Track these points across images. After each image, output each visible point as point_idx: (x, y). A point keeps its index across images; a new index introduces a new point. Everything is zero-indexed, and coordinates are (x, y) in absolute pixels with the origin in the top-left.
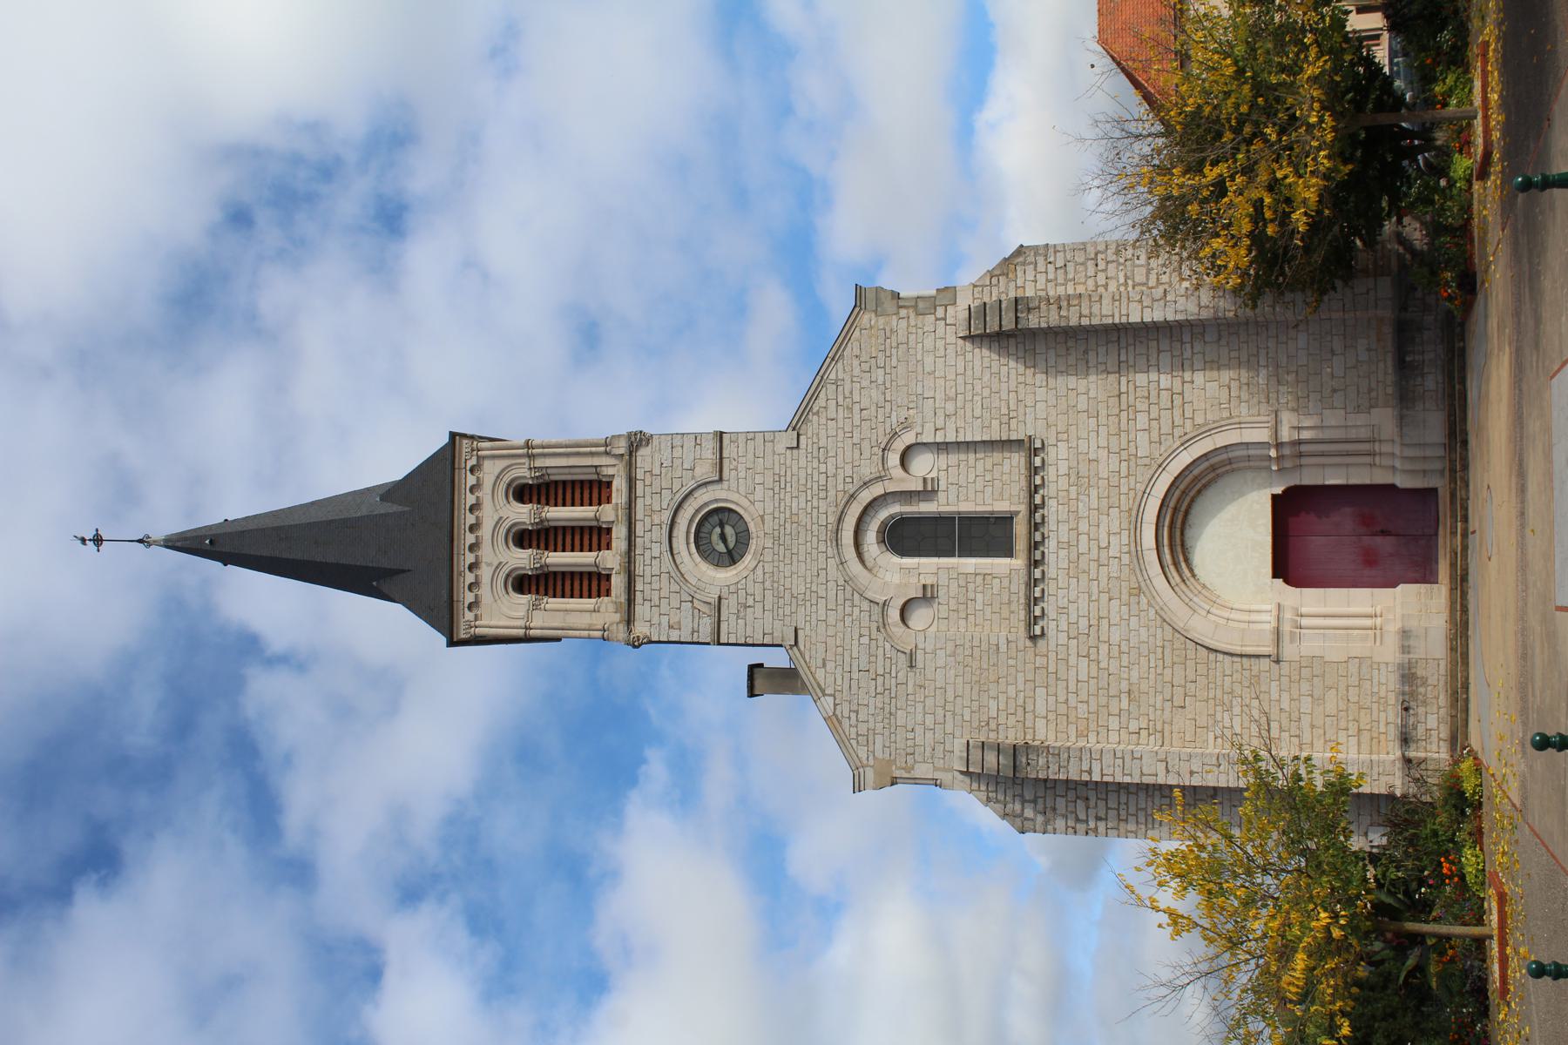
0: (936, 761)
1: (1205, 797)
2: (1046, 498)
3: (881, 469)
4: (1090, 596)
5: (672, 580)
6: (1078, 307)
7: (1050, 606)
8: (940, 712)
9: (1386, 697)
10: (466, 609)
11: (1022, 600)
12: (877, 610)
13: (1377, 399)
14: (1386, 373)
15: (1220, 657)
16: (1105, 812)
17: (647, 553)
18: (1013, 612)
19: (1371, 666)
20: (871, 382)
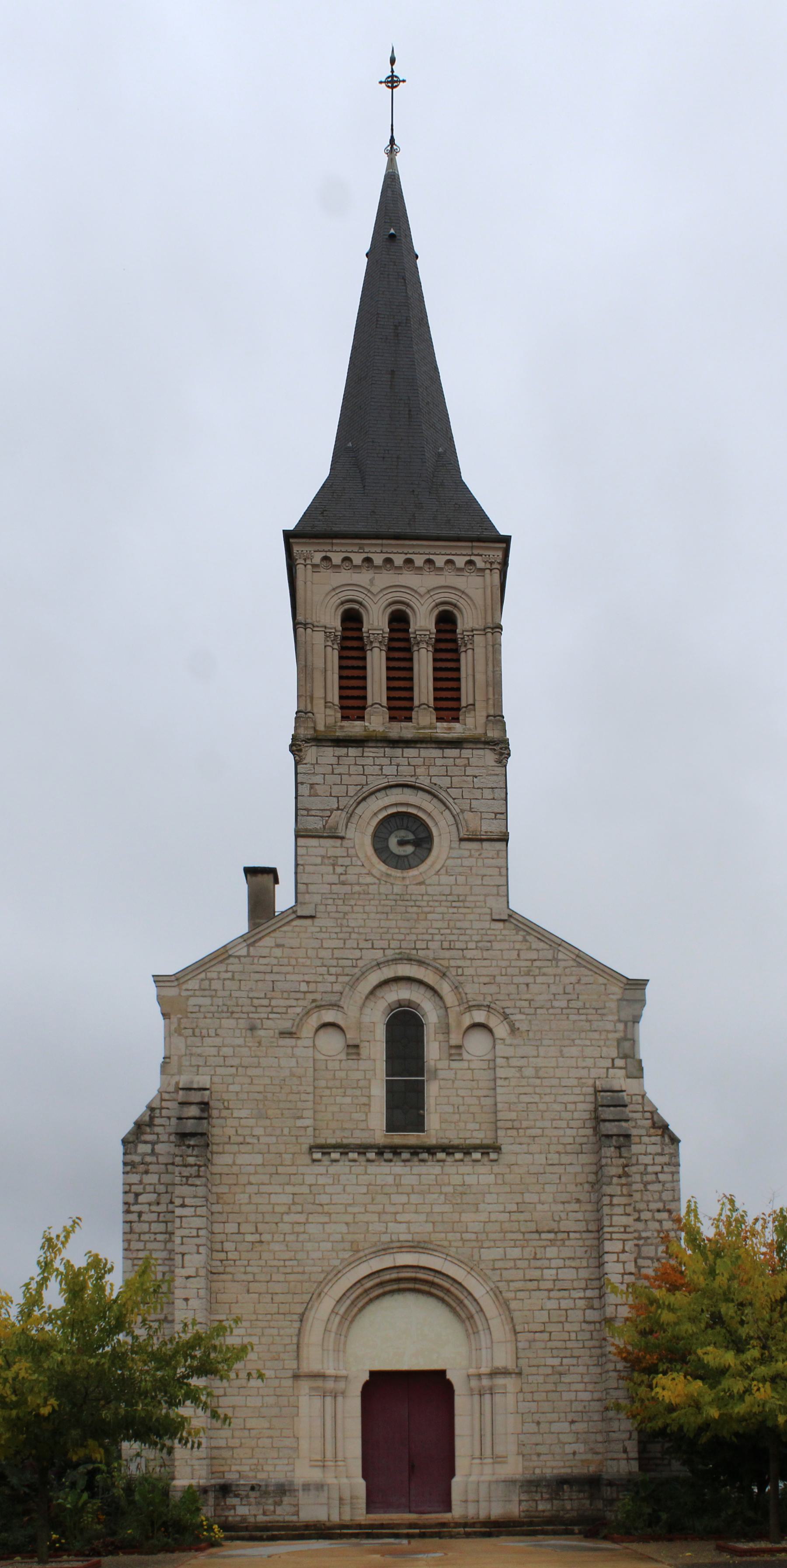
0: (188, 1058)
1: (165, 1312)
2: (441, 1164)
3: (471, 1003)
4: (350, 1205)
5: (359, 787)
8: (236, 1062)
11: (345, 1141)
12: (334, 998)
13: (531, 1460)
14: (553, 1468)
17: (386, 761)
18: (334, 1132)
20: (554, 995)
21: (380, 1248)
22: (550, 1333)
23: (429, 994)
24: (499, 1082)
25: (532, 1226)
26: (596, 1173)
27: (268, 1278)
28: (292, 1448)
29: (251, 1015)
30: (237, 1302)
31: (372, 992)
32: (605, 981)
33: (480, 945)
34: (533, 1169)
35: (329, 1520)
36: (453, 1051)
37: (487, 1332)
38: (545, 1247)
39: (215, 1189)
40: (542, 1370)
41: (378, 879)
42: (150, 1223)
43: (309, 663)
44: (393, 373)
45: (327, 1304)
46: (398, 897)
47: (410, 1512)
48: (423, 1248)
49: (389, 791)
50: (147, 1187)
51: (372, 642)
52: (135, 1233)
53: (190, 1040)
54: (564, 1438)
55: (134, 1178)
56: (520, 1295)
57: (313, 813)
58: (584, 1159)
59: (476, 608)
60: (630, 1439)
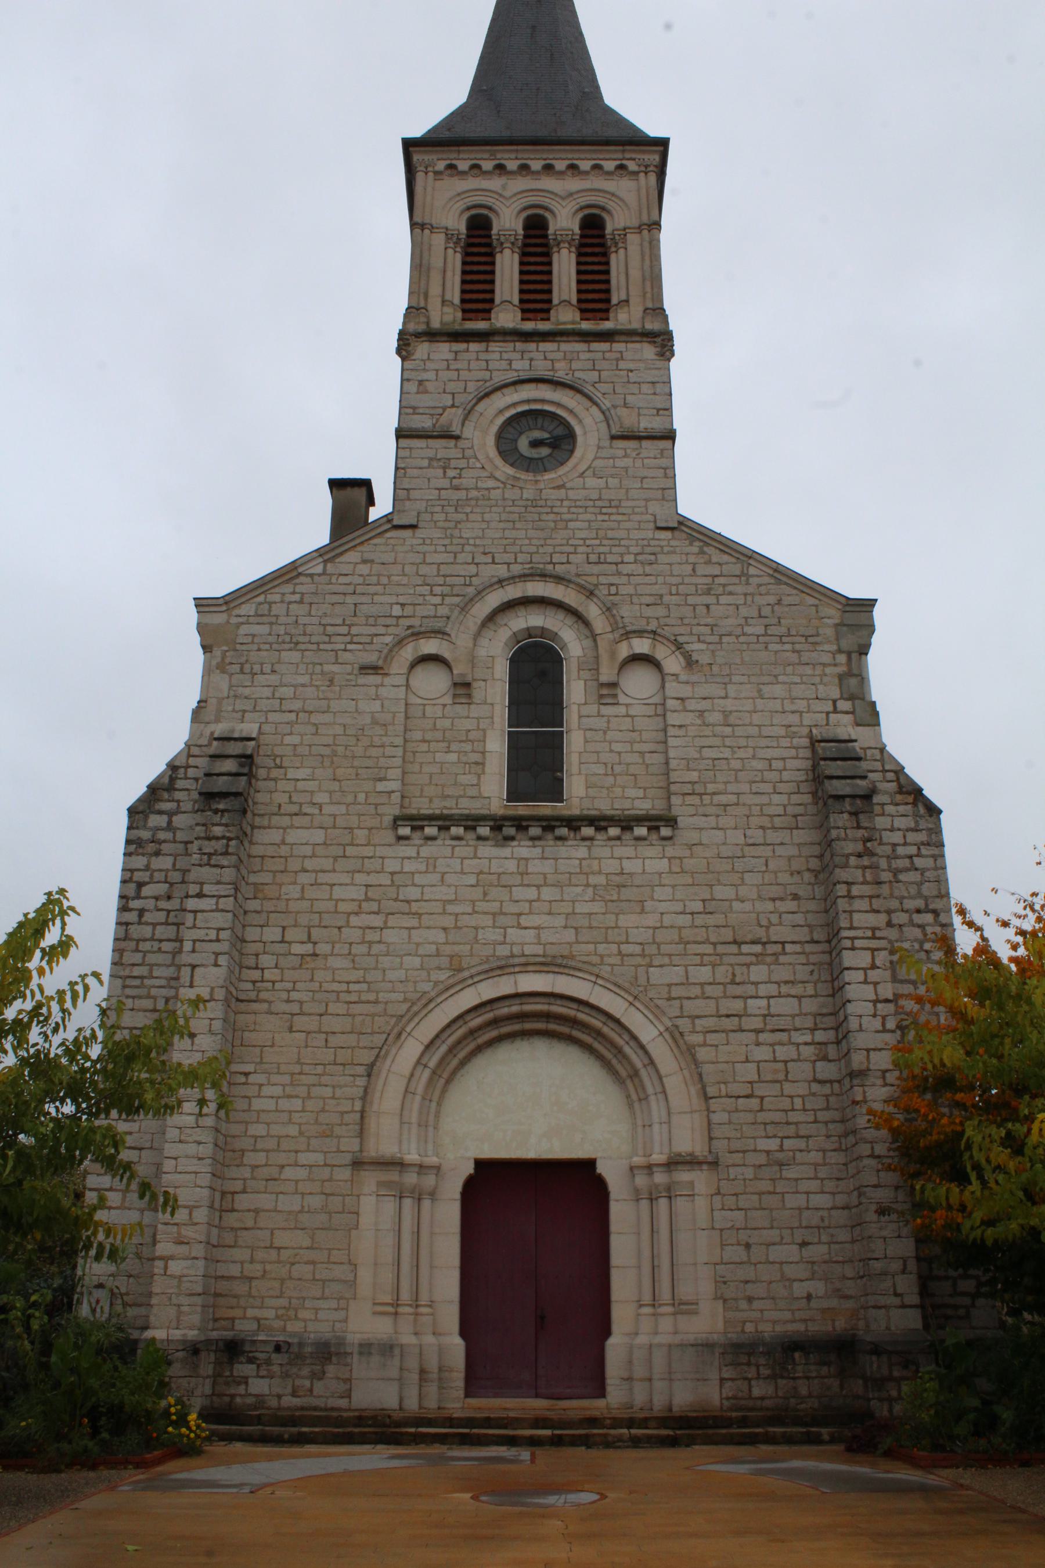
0: (231, 700)
2: (588, 843)
3: (628, 629)
4: (450, 902)
5: (481, 383)
6: (861, 879)
7: (440, 848)
8: (297, 705)
9: (296, 1318)
10: (448, 162)
12: (438, 624)
13: (737, 1309)
14: (774, 1322)
15: (361, 1082)
16: (150, 921)
17: (518, 356)
18: (431, 801)
19: (342, 1298)
20: (746, 618)
21: (494, 965)
22: (762, 1098)
23: (570, 620)
24: (671, 731)
25: (727, 935)
26: (821, 857)
27: (322, 1010)
28: (345, 1282)
29: (322, 646)
30: (272, 1046)
31: (491, 618)
32: (817, 602)
33: (640, 558)
34: (726, 851)
35: (401, 1409)
36: (605, 691)
37: (661, 1096)
38: (748, 965)
39: (252, 879)
40: (752, 1159)
41: (503, 483)
42: (154, 925)
43: (425, 262)
44: (534, 27)
45: (411, 1050)
46: (529, 503)
47: (537, 1396)
48: (560, 966)
49: (519, 387)
50: (156, 874)
51: (502, 244)
52: (131, 939)
53: (237, 679)
54: (790, 1271)
55: (140, 862)
56: (711, 1038)
57: (421, 411)
58: (800, 836)
59: (629, 209)
60: (903, 1272)
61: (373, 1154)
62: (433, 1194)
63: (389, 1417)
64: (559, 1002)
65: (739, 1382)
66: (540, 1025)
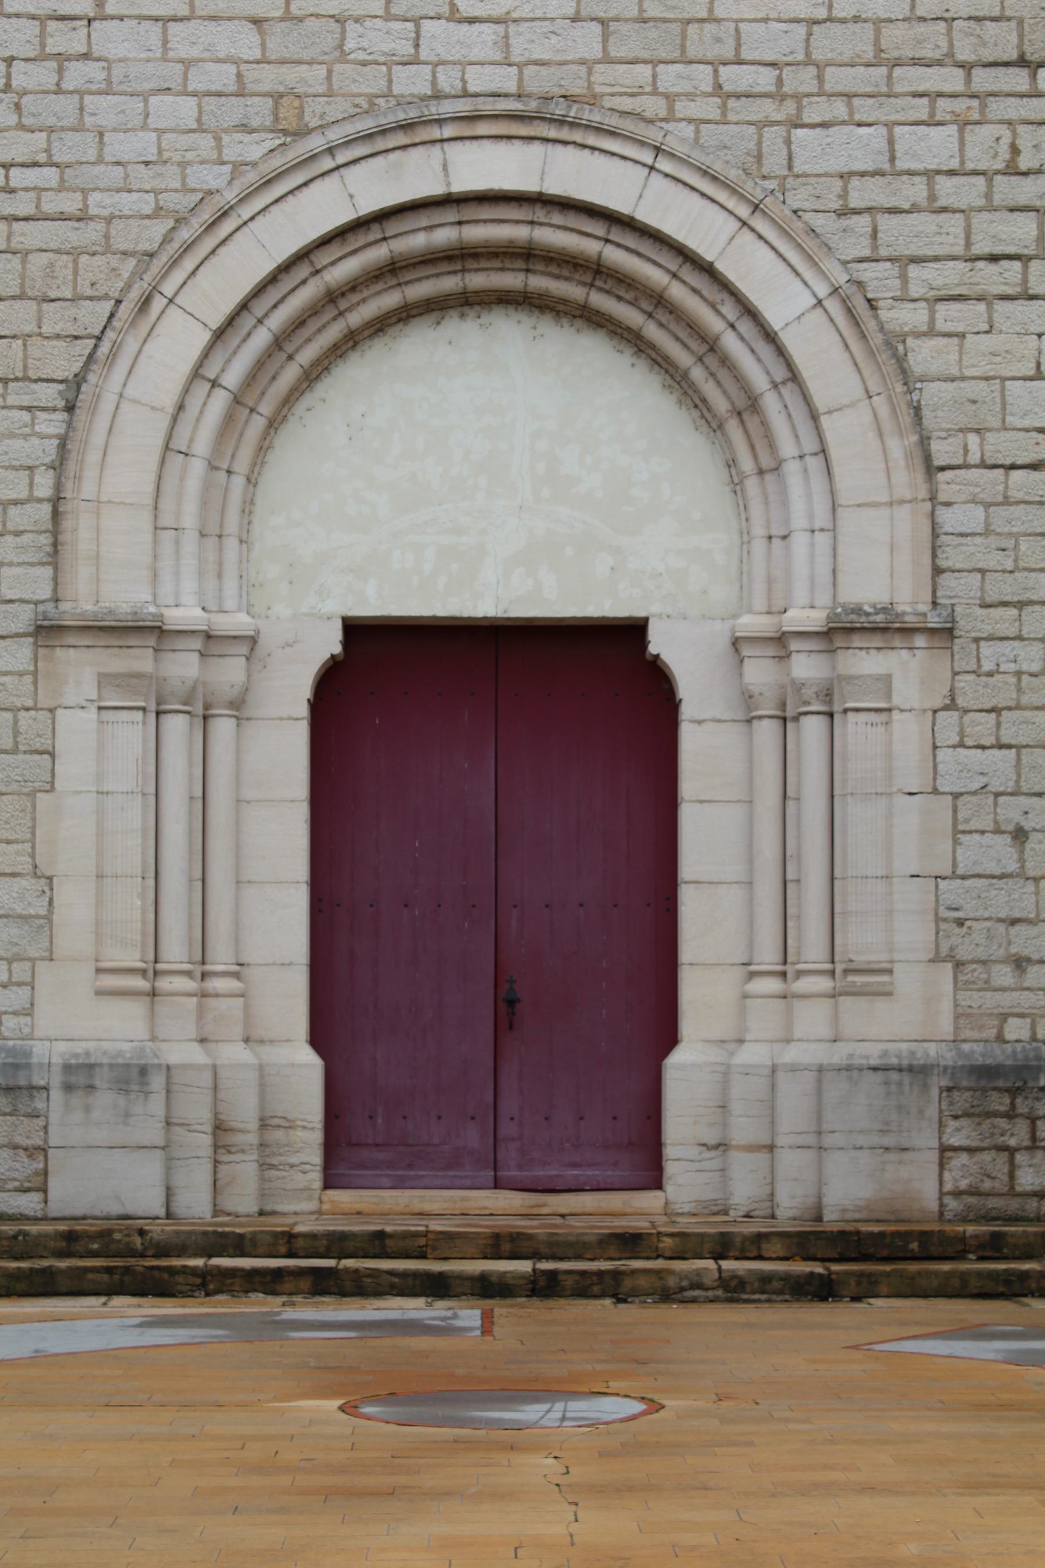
13: (988, 987)
15: (52, 424)
28: (25, 918)
35: (169, 1215)
37: (814, 464)
47: (497, 1185)
48: (561, 122)
61: (88, 607)
62: (238, 705)
63: (142, 1232)
64: (557, 218)
65: (986, 1157)
66: (511, 280)
